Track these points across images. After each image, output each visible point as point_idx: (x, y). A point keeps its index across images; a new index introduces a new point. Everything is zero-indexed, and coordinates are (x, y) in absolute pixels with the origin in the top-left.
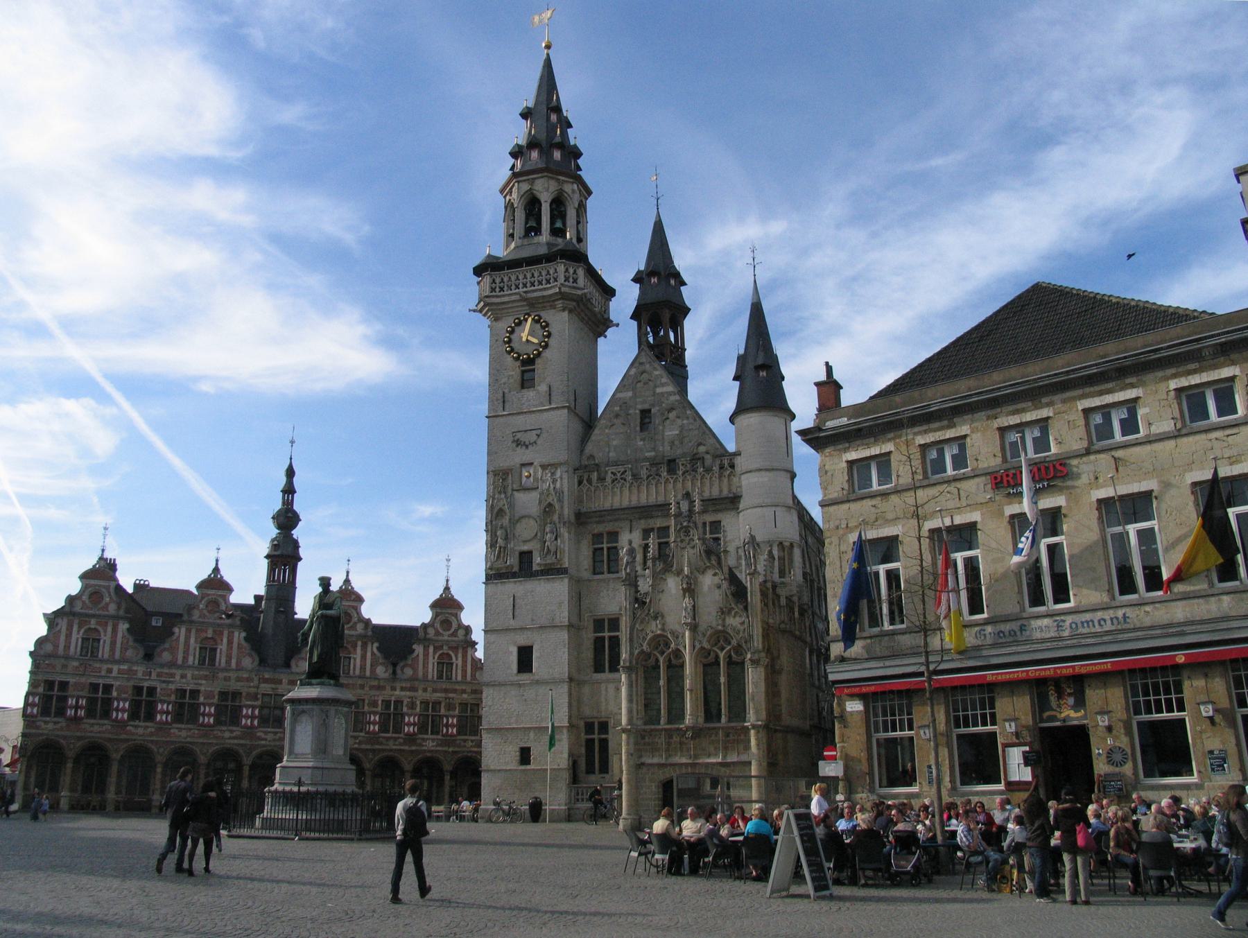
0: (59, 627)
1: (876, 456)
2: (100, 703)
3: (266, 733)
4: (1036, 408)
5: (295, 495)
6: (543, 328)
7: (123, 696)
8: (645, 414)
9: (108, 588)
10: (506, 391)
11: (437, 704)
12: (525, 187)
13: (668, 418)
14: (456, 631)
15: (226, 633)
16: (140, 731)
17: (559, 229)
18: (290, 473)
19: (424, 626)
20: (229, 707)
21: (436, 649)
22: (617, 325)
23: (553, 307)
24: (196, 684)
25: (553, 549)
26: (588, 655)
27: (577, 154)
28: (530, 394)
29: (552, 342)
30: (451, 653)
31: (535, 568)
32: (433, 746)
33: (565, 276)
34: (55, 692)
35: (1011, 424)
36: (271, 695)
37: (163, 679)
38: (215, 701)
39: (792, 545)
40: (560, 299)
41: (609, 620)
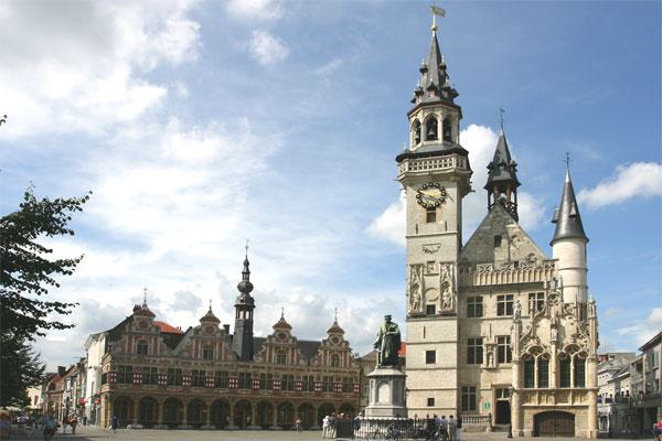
2: (151, 378)
23: (448, 180)
26: (465, 355)
27: (453, 94)
31: (437, 313)
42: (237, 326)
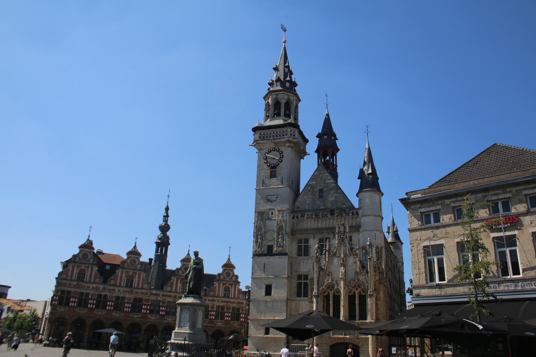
0: (68, 268)
1: (433, 211)
2: (83, 301)
3: (152, 316)
4: (504, 193)
5: (169, 218)
6: (280, 154)
7: (94, 298)
8: (321, 191)
9: (90, 252)
10: (264, 179)
11: (223, 307)
12: (274, 96)
13: (330, 193)
14: (232, 277)
15: (137, 274)
16: (100, 313)
17: (288, 114)
18: (167, 209)
19: (219, 274)
20: (137, 305)
21: (224, 284)
22: (309, 154)
23: (285, 146)
24: (124, 294)
25: (282, 245)
26: (295, 289)
27: (294, 84)
28: (274, 180)
29: (284, 159)
30: (229, 286)
31: (273, 252)
32: (220, 325)
33: (290, 133)
34: (65, 295)
35: (493, 199)
36: (155, 300)
37: (111, 291)
38: (132, 301)
39: (382, 247)
40: (288, 142)
41: (304, 275)
42: (155, 261)
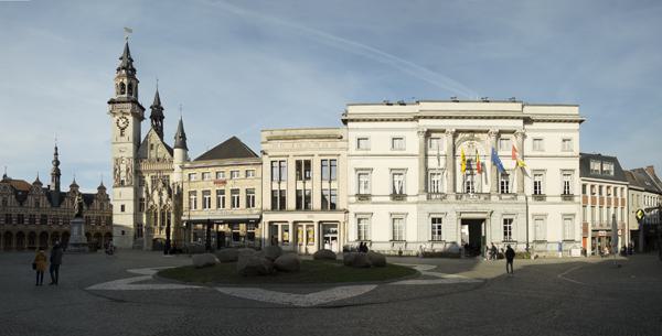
18: (56, 149)
20: (44, 220)
